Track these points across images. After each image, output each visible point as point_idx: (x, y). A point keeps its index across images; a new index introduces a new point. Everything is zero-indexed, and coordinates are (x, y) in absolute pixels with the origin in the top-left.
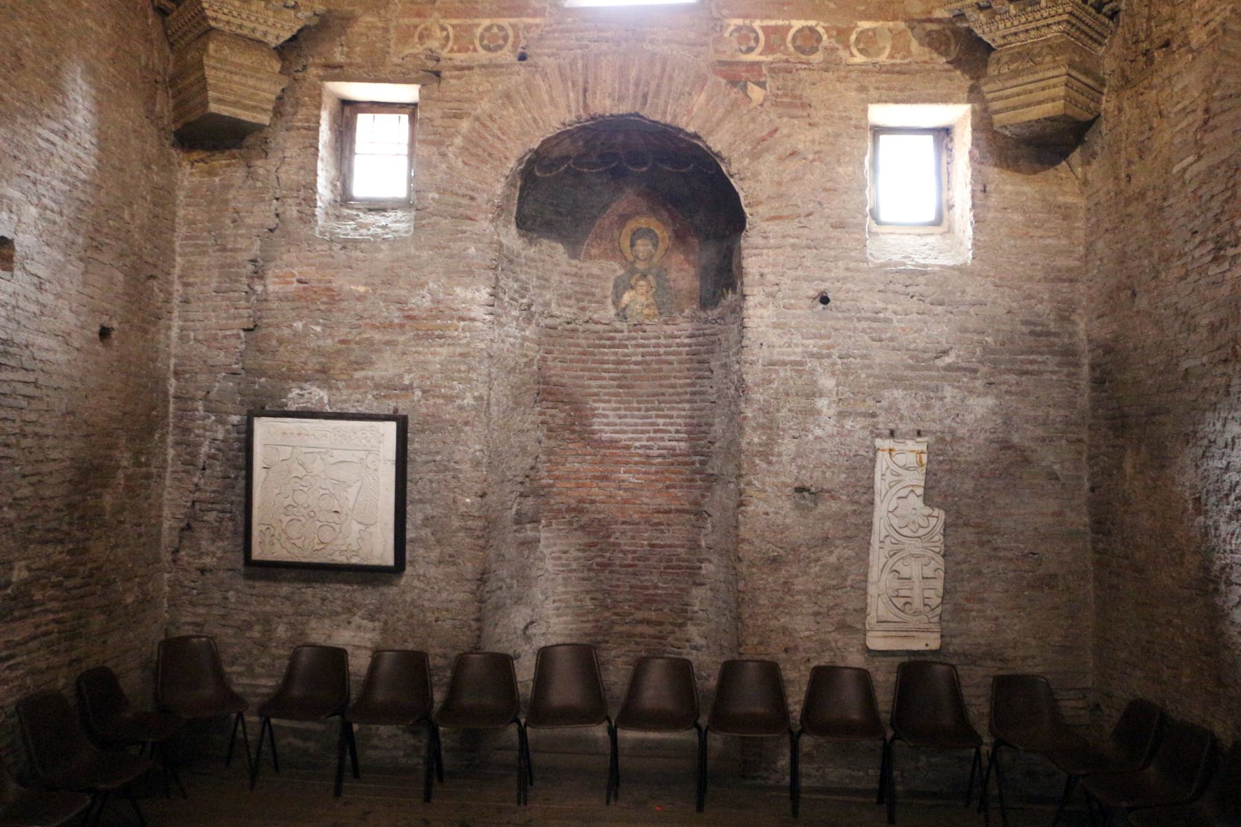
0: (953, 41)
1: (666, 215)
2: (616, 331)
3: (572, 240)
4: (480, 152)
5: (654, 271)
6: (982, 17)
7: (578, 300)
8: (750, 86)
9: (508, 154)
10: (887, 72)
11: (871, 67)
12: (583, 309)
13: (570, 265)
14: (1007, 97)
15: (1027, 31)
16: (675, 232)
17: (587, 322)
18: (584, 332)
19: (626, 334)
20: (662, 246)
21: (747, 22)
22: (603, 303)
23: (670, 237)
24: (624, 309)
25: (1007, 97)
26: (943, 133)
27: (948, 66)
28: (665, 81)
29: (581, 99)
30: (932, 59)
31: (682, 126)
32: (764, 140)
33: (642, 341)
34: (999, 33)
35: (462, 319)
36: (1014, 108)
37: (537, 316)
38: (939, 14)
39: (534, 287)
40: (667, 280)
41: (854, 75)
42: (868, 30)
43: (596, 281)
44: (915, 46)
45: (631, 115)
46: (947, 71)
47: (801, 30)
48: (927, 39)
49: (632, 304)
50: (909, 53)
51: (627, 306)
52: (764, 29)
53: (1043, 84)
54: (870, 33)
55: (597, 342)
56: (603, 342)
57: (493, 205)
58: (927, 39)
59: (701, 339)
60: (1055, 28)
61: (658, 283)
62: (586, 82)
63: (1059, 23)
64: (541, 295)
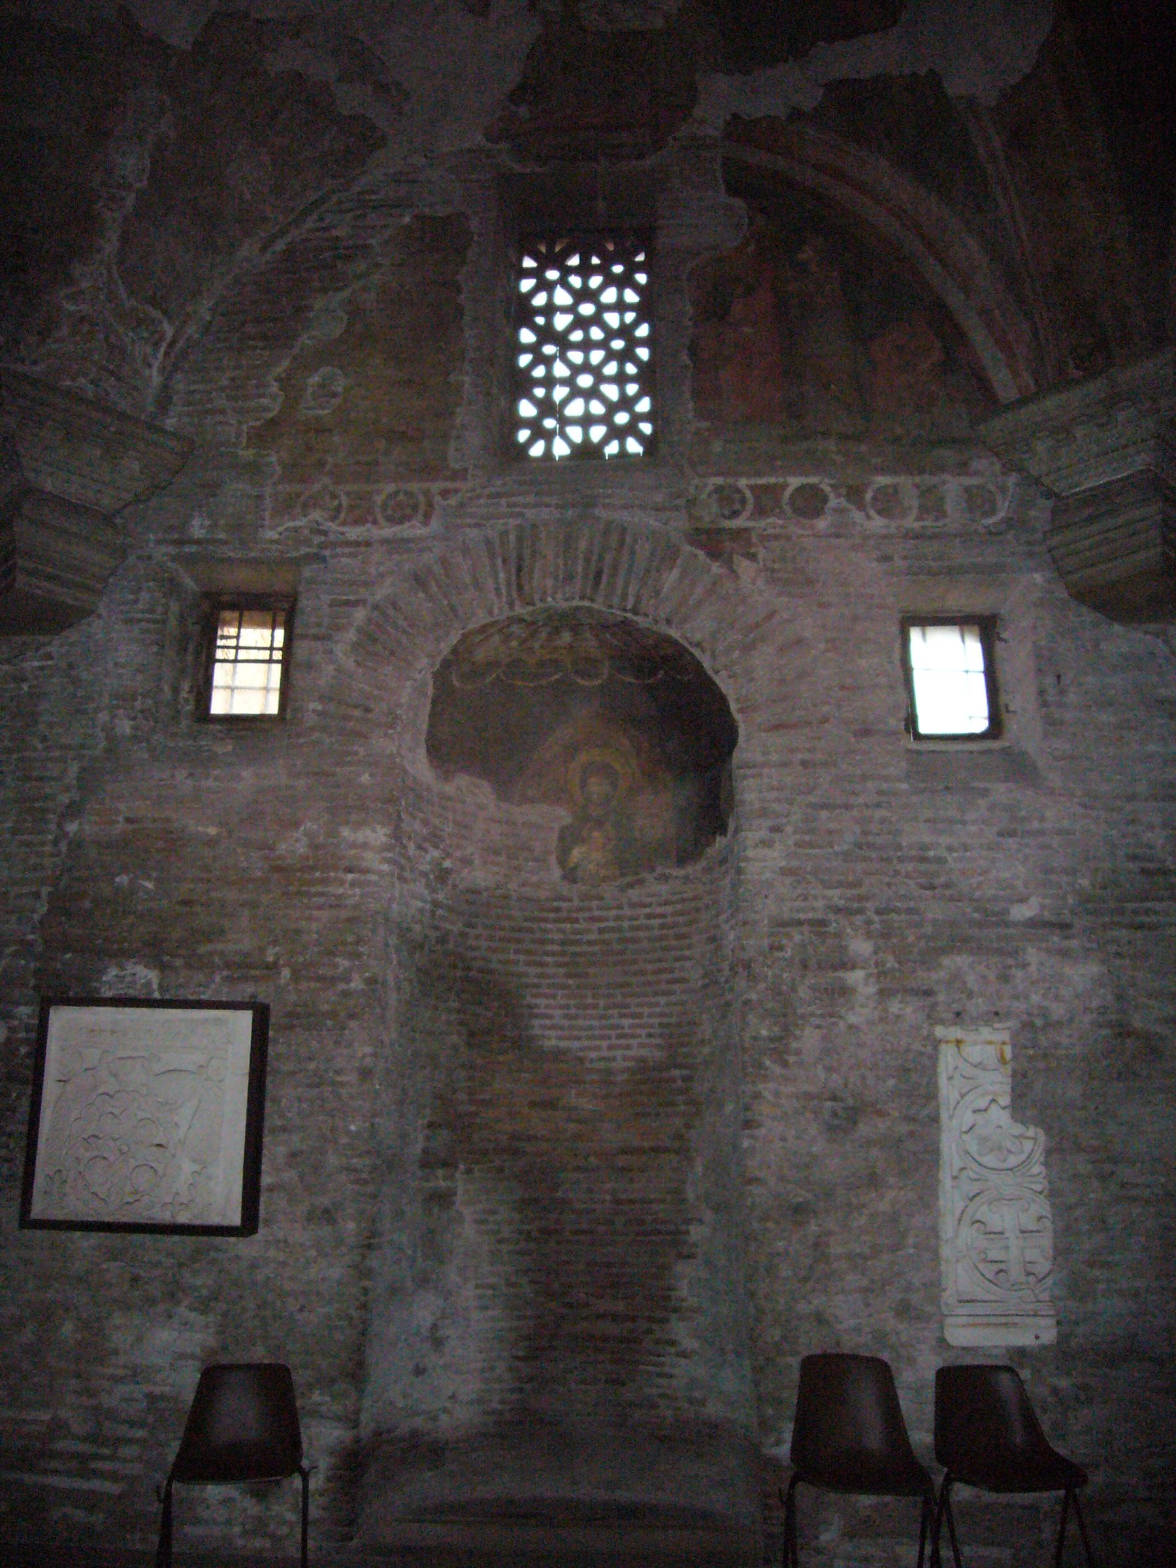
8: (736, 558)
21: (730, 481)
28: (625, 557)
29: (514, 578)
32: (757, 625)
35: (349, 870)
47: (801, 489)
51: (577, 865)
52: (752, 488)
62: (520, 558)
64: (458, 847)
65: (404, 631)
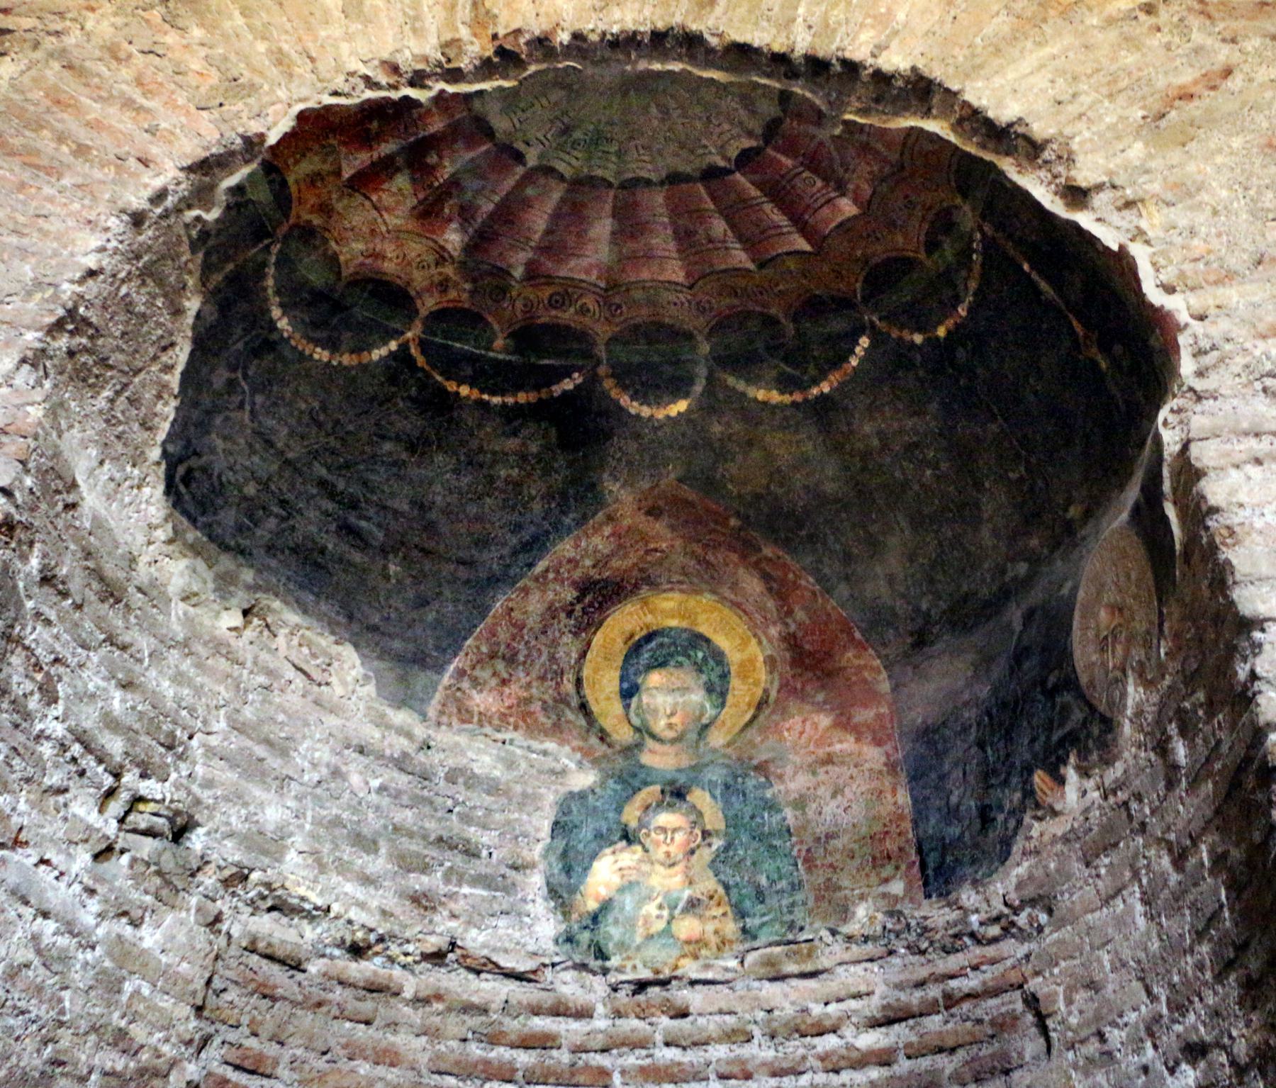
1: (753, 585)
2: (559, 1010)
3: (397, 644)
4: (45, 141)
5: (716, 775)
7: (409, 865)
9: (155, 150)
12: (422, 902)
13: (381, 722)
16: (791, 641)
17: (436, 957)
18: (420, 1001)
19: (600, 1023)
20: (742, 693)
22: (510, 889)
23: (771, 662)
24: (595, 918)
31: (859, 51)
33: (672, 1054)
37: (209, 880)
39: (210, 751)
40: (772, 806)
43: (488, 800)
45: (659, 41)
49: (628, 901)
51: (606, 906)
55: (476, 1051)
56: (502, 1053)
57: (55, 297)
59: (934, 1023)
61: (733, 822)
64: (238, 797)
65: (128, 104)
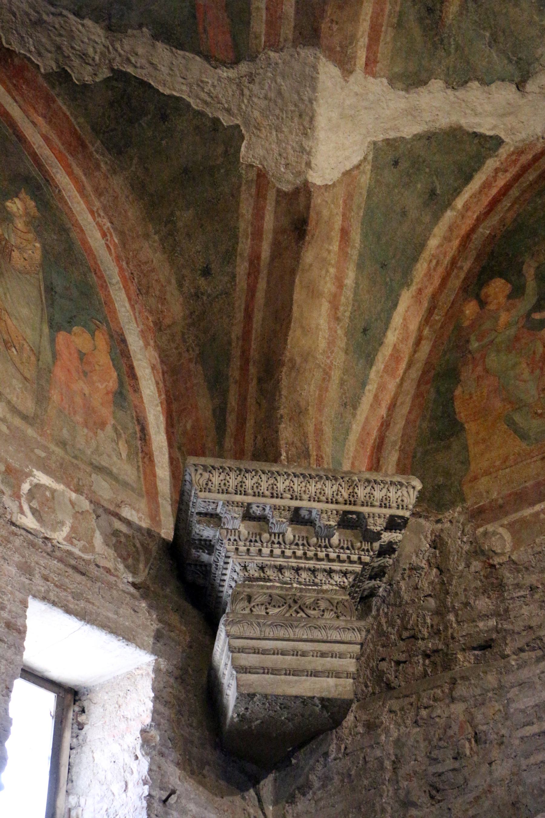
0: (142, 558)
6: (243, 528)
10: (61, 560)
11: (40, 541)
14: (264, 652)
15: (297, 570)
25: (264, 652)
26: (69, 697)
27: (132, 590)
30: (116, 570)
34: (259, 560)
36: (274, 671)
38: (127, 513)
41: (18, 542)
42: (46, 488)
44: (98, 540)
46: (132, 595)
48: (114, 540)
50: (89, 548)
53: (324, 647)
54: (48, 494)
58: (114, 540)
60: (337, 578)
63: (345, 574)
